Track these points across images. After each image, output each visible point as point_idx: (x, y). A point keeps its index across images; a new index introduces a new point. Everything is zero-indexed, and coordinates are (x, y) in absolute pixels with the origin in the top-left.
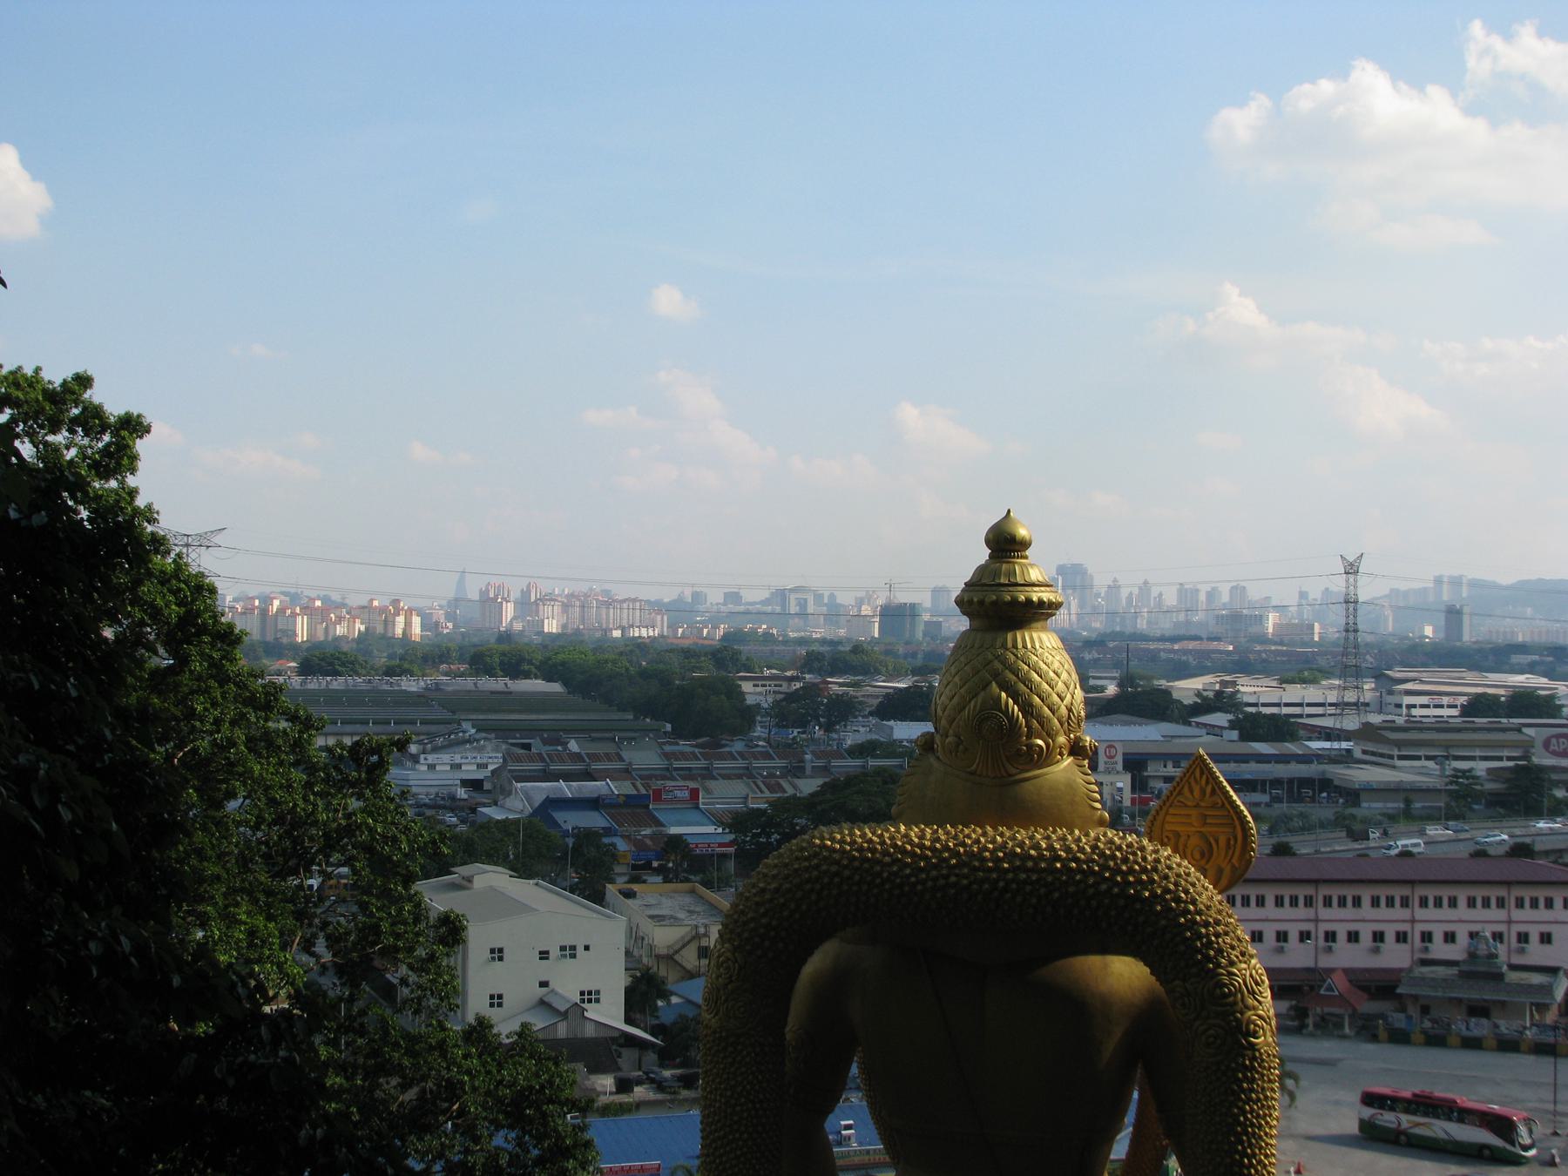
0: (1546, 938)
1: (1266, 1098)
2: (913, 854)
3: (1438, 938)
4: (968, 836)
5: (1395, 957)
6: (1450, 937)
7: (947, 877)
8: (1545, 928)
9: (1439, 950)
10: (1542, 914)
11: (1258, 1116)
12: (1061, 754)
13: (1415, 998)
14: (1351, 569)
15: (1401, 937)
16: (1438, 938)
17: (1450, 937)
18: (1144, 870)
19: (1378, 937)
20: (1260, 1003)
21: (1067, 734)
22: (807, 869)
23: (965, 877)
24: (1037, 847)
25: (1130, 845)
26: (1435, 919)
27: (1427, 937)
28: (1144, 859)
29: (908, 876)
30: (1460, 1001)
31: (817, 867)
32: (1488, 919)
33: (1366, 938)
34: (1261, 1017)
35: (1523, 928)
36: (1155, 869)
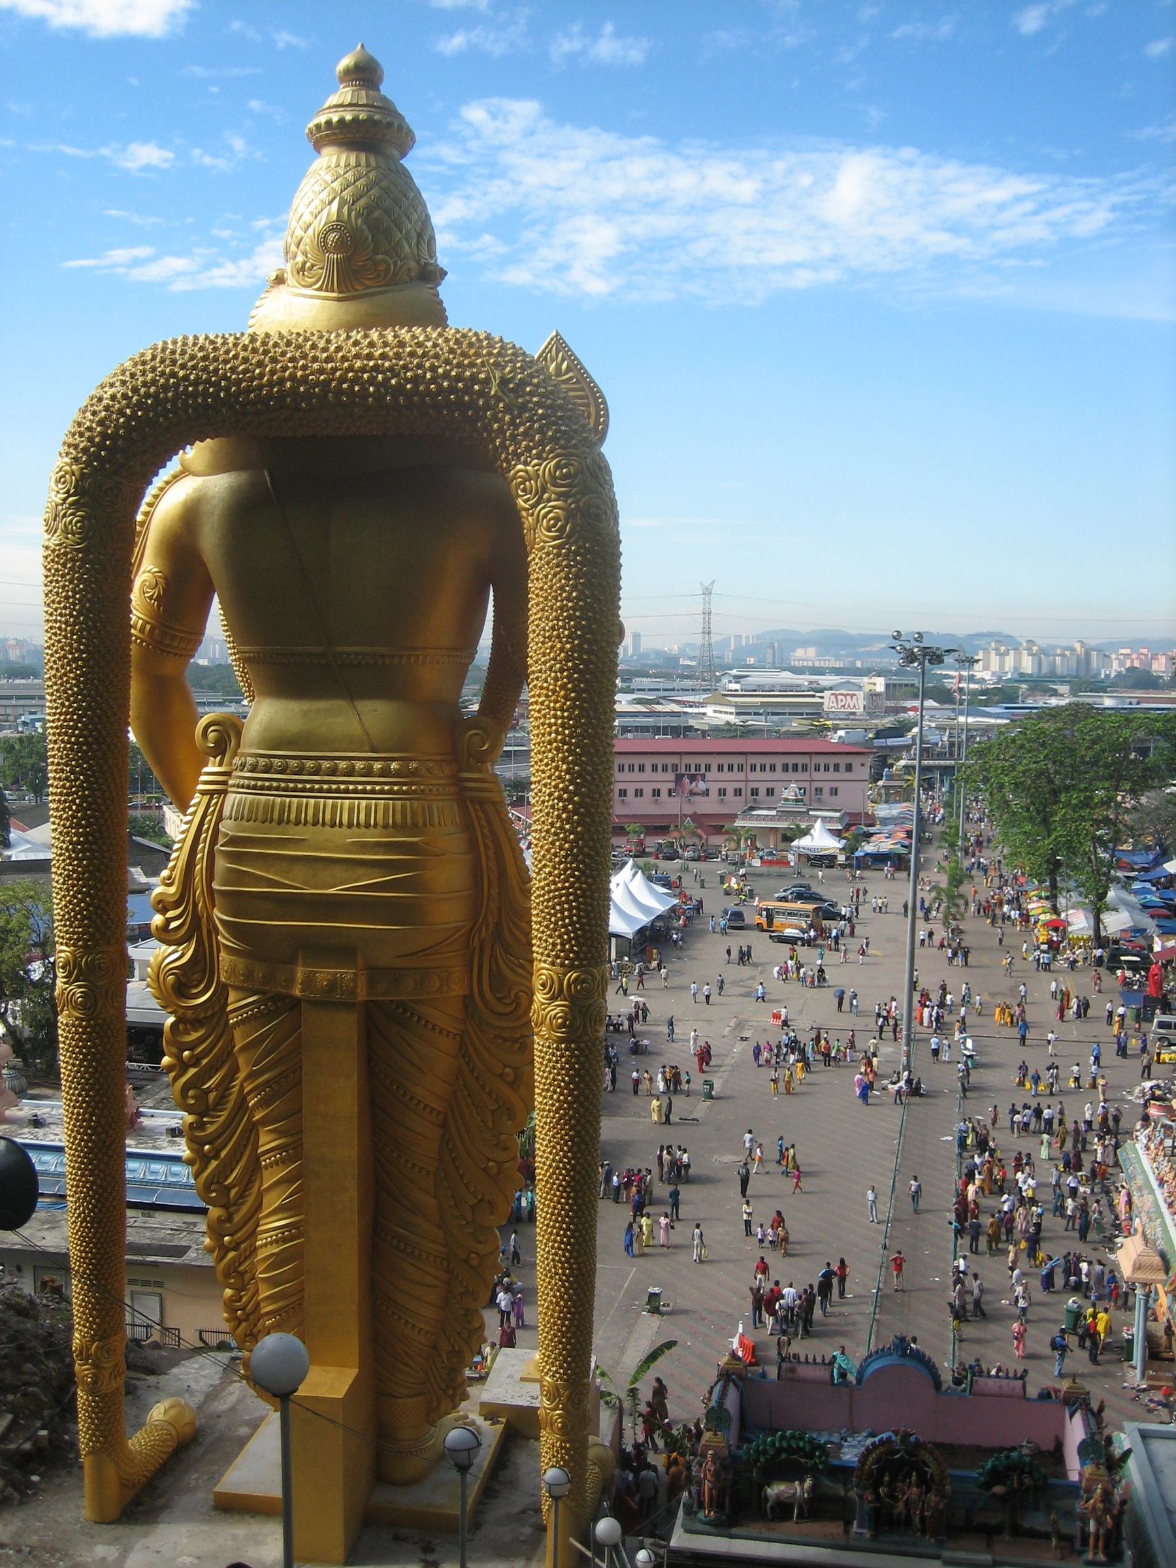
0: (834, 792)
10: (831, 775)
14: (707, 592)
15: (738, 792)
19: (722, 792)
35: (818, 785)
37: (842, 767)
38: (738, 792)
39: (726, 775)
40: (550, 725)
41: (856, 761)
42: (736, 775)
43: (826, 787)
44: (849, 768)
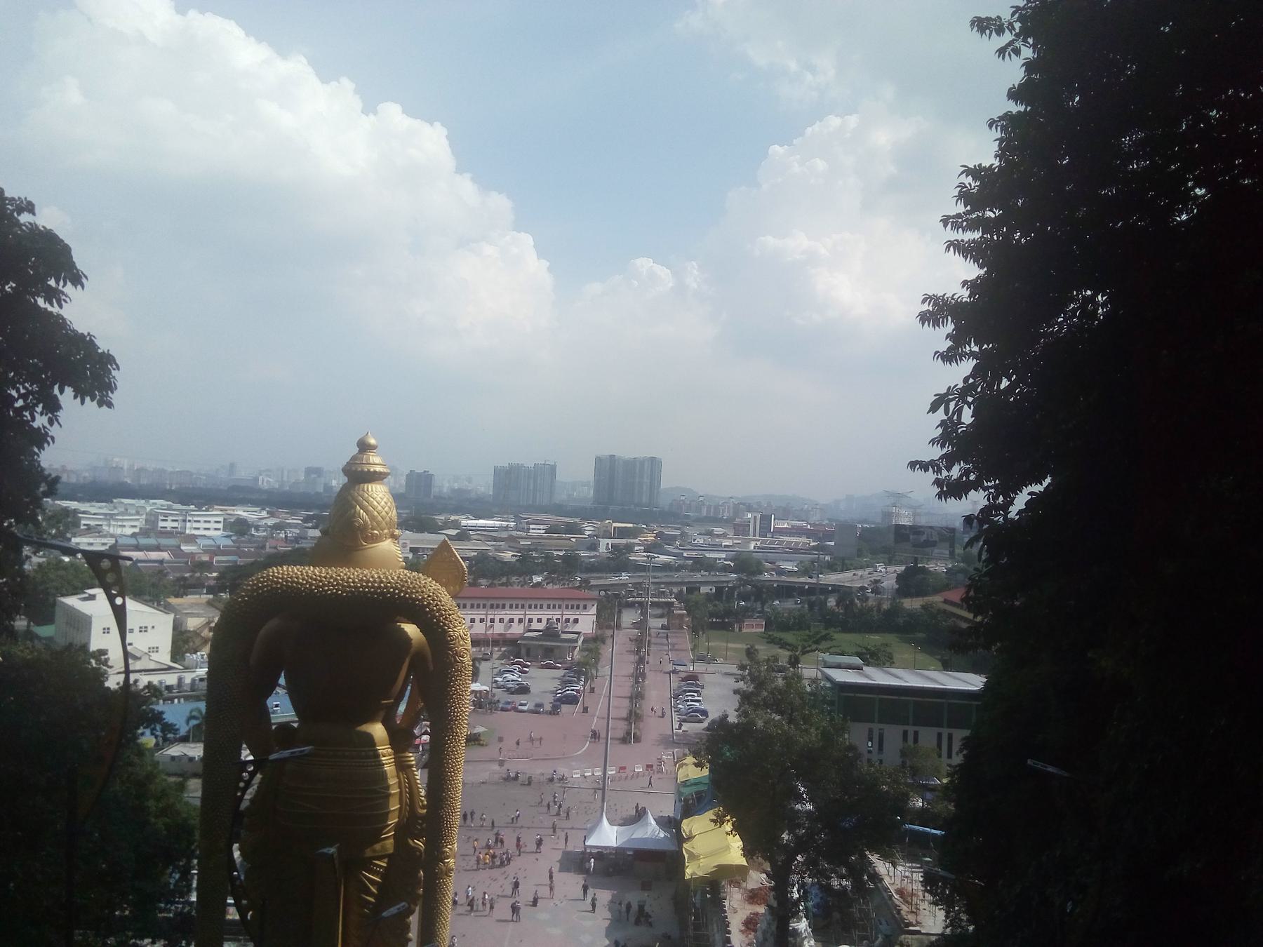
1: (466, 683)
2: (316, 580)
3: (535, 620)
4: (341, 572)
5: (517, 629)
6: (539, 621)
9: (535, 626)
11: (462, 691)
12: (386, 537)
16: (535, 620)
17: (539, 621)
18: (420, 587)
24: (373, 577)
25: (414, 577)
26: (534, 614)
27: (530, 621)
28: (420, 582)
32: (555, 614)
34: (466, 649)
36: (424, 587)
38: (520, 621)
41: (589, 604)
44: (585, 607)
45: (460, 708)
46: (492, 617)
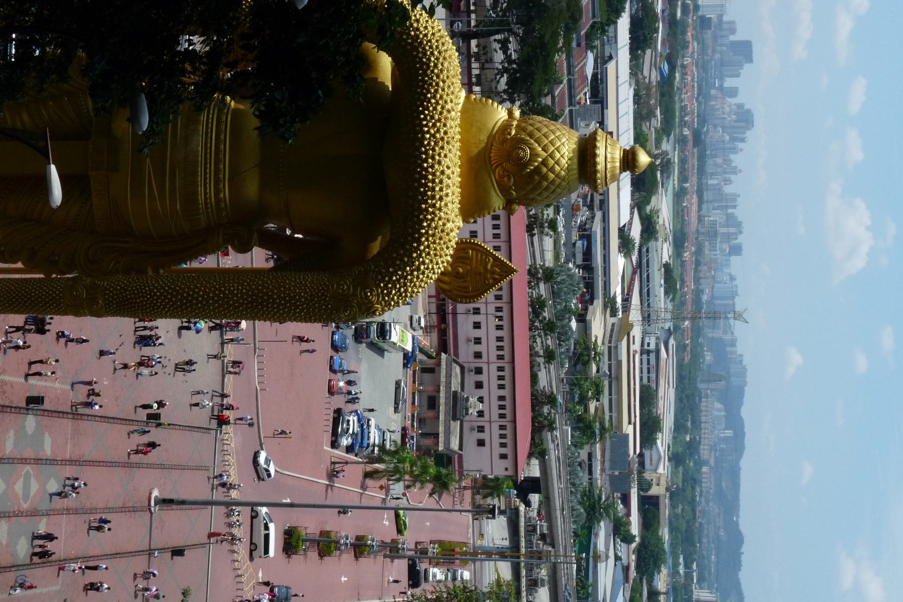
0: (481, 443)
2: (441, 113)
7: (428, 132)
8: (487, 442)
10: (496, 441)
13: (439, 364)
16: (479, 378)
19: (478, 341)
20: (363, 314)
21: (518, 198)
22: (431, 47)
23: (429, 144)
27: (479, 371)
29: (428, 109)
30: (438, 391)
31: (432, 53)
33: (477, 333)
35: (487, 429)
37: (503, 451)
38: (478, 355)
39: (494, 344)
40: (233, 286)
41: (508, 463)
42: (494, 353)
43: (484, 436)
44: (503, 456)
45: (278, 311)
46: (483, 311)
